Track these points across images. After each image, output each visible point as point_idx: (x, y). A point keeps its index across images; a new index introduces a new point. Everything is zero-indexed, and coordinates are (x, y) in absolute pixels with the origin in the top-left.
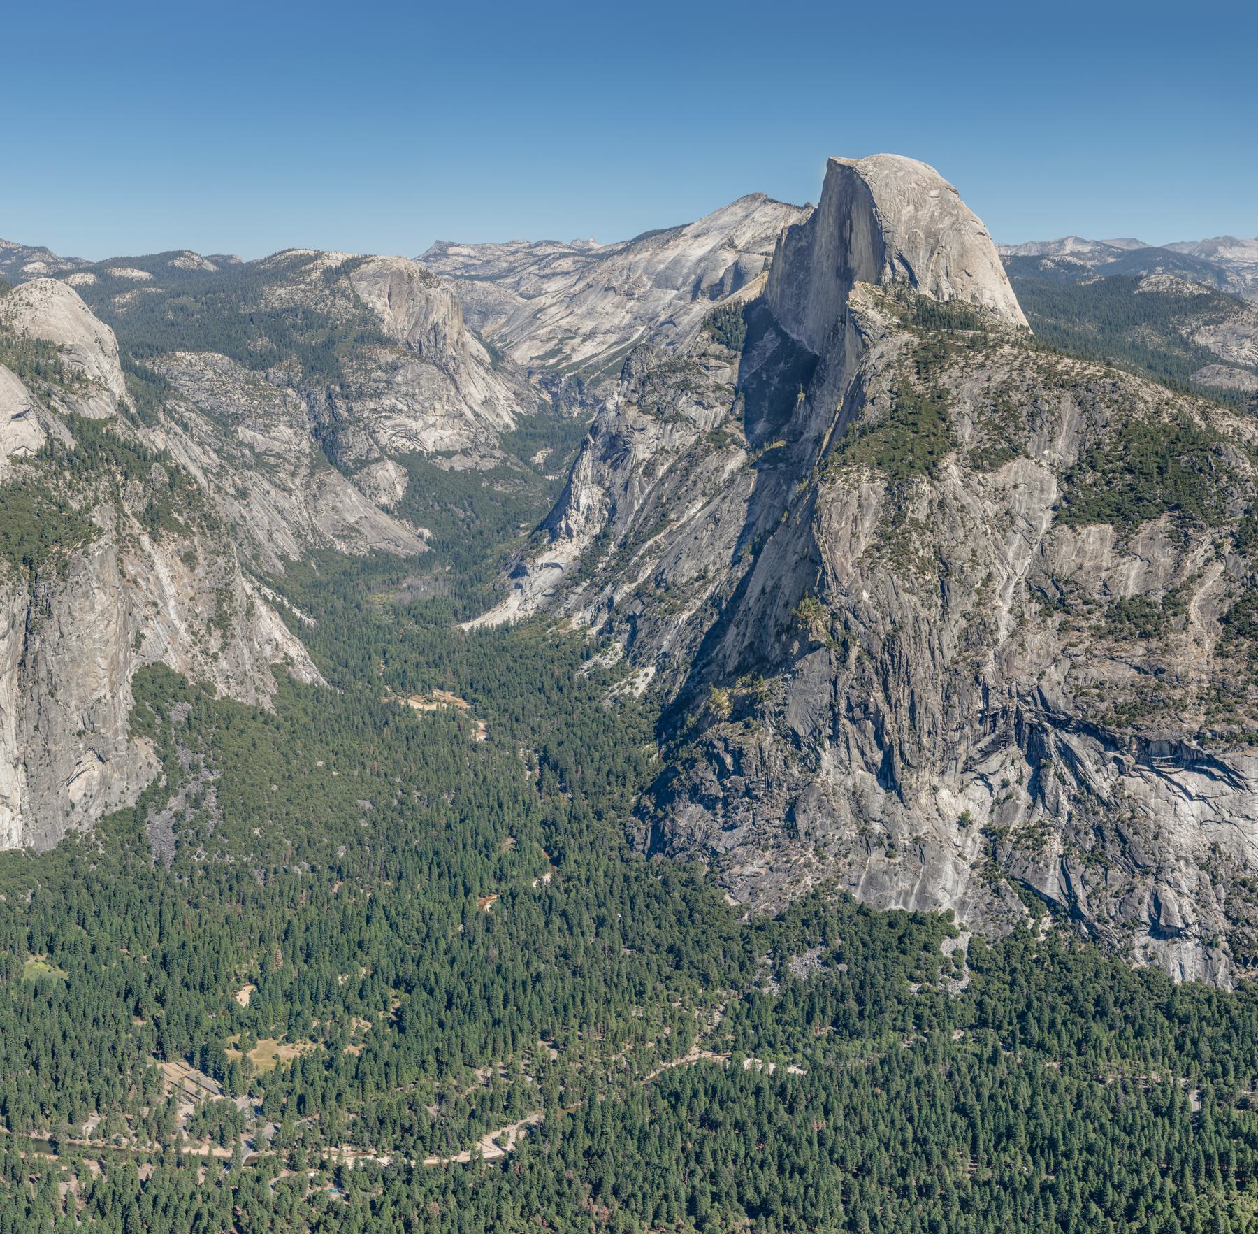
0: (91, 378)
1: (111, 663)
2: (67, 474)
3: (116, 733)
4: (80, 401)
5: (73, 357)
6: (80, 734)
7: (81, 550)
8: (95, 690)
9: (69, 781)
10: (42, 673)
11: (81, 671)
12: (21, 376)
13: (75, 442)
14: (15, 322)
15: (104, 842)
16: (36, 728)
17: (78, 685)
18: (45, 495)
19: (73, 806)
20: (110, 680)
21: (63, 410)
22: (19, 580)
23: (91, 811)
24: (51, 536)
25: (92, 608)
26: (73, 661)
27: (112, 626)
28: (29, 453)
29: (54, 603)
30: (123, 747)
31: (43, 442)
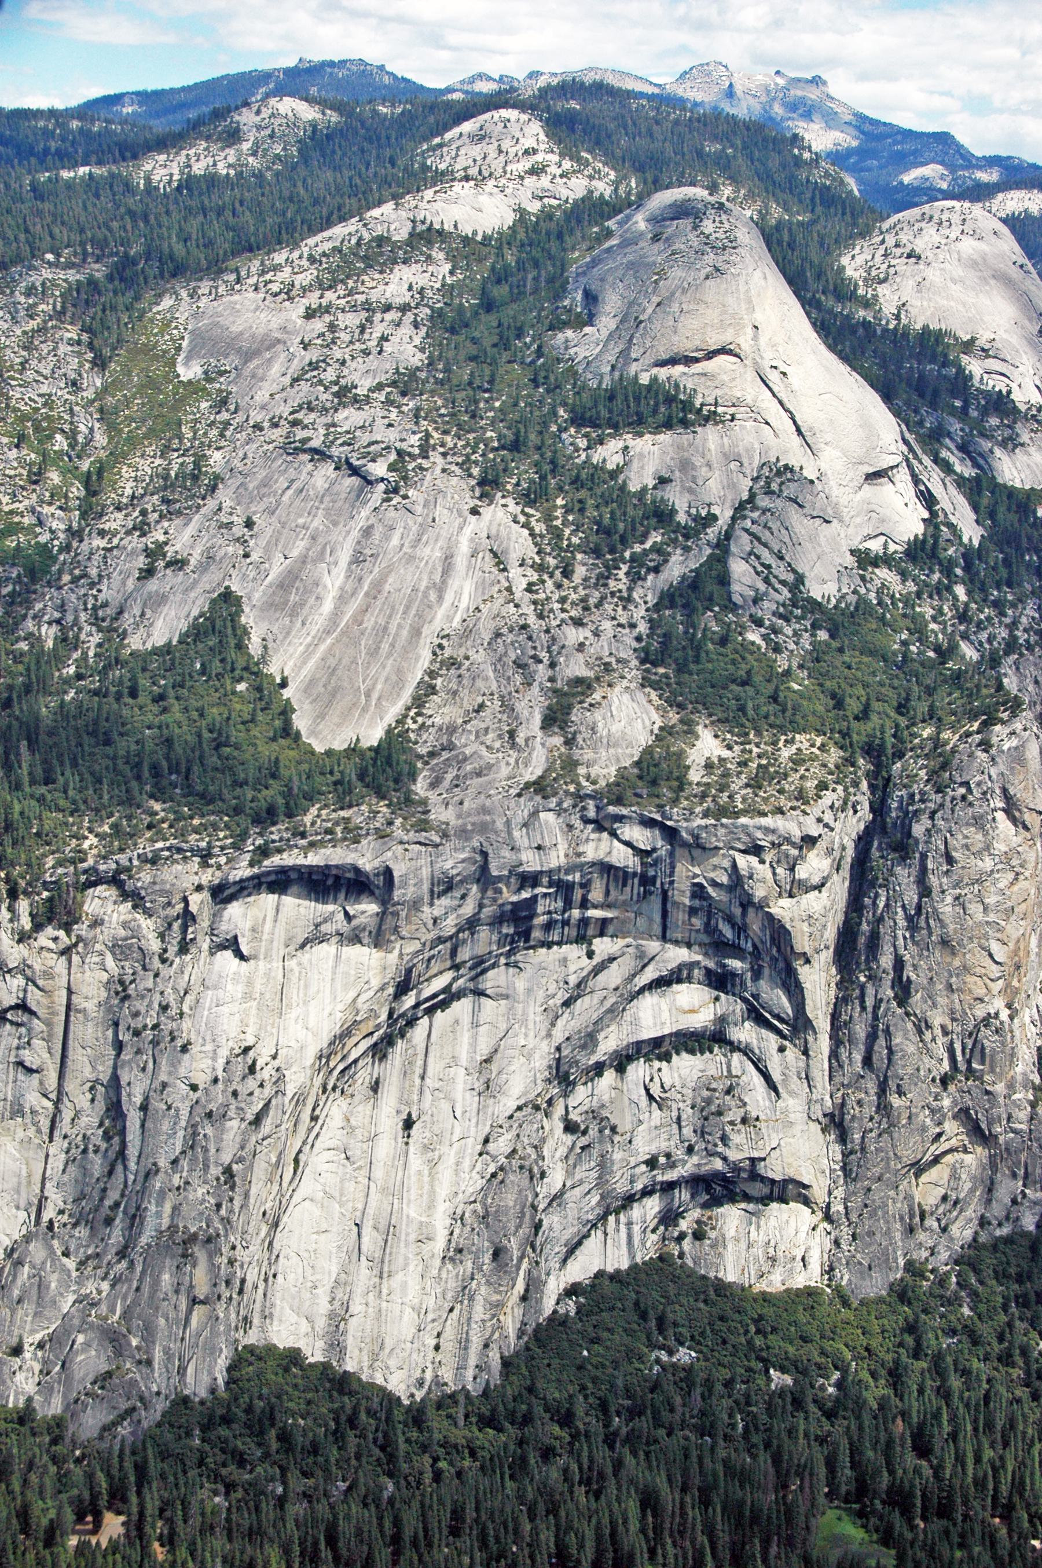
0: (1023, 408)
1: (1016, 952)
2: (960, 591)
3: (1011, 1087)
4: (998, 452)
5: (993, 364)
6: (945, 1081)
7: (978, 738)
8: (981, 1000)
9: (919, 1168)
10: (886, 961)
11: (957, 963)
12: (887, 396)
13: (981, 531)
14: (882, 290)
15: (974, 1294)
16: (867, 1061)
17: (950, 987)
18: (919, 630)
19: (923, 1216)
20: (1008, 985)
21: (967, 471)
22: (856, 784)
23: (955, 1230)
24: (922, 708)
25: (988, 847)
26: (945, 943)
27: (1022, 884)
28: (892, 547)
29: (918, 830)
30: (1023, 1115)
31: (919, 529)
